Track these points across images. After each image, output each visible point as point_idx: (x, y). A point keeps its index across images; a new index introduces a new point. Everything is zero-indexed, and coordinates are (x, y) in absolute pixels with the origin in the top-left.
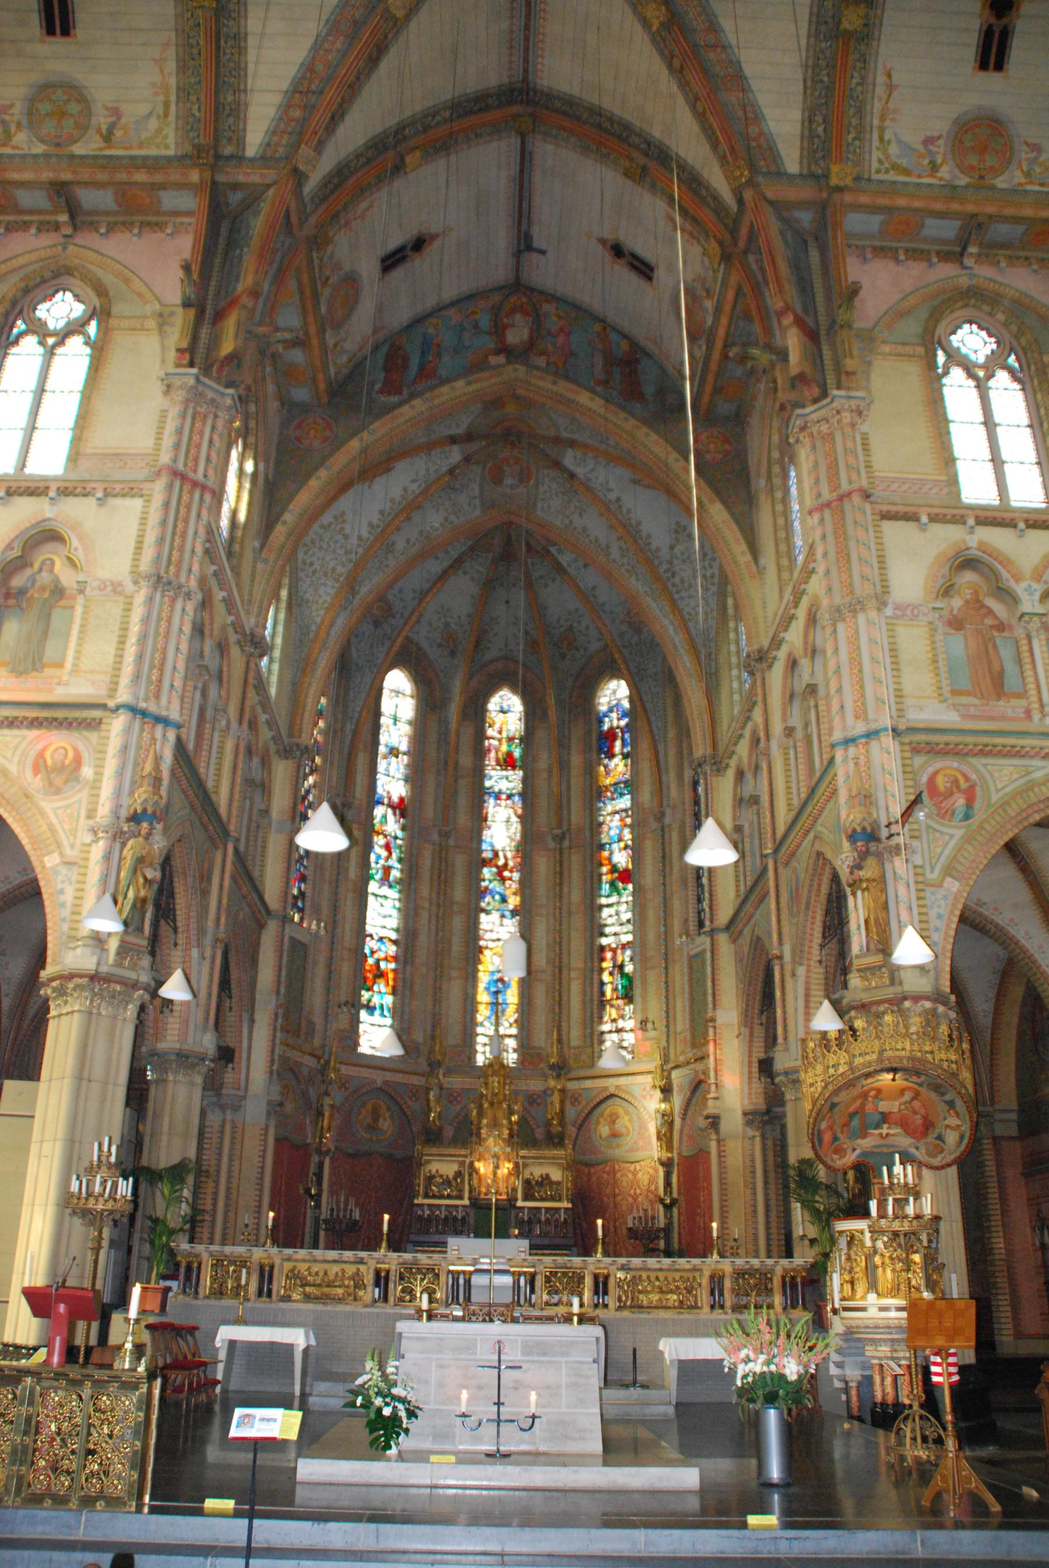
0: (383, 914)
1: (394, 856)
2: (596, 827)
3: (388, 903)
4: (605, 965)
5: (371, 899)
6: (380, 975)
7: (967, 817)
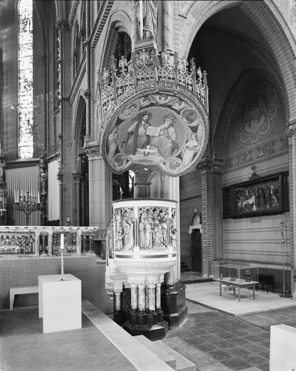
4: (21, 120)
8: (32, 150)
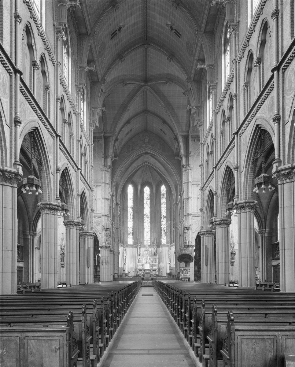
0: (130, 224)
2: (160, 209)
5: (129, 222)
8: (166, 241)
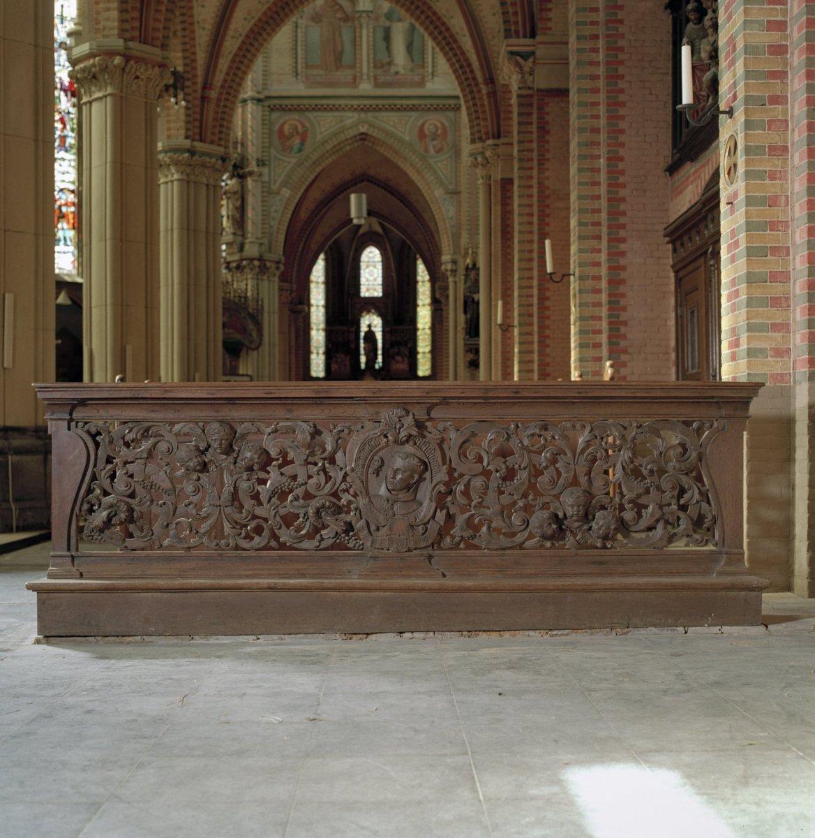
1: (68, 127)
3: (66, 163)
6: (63, 216)
7: (300, 150)
